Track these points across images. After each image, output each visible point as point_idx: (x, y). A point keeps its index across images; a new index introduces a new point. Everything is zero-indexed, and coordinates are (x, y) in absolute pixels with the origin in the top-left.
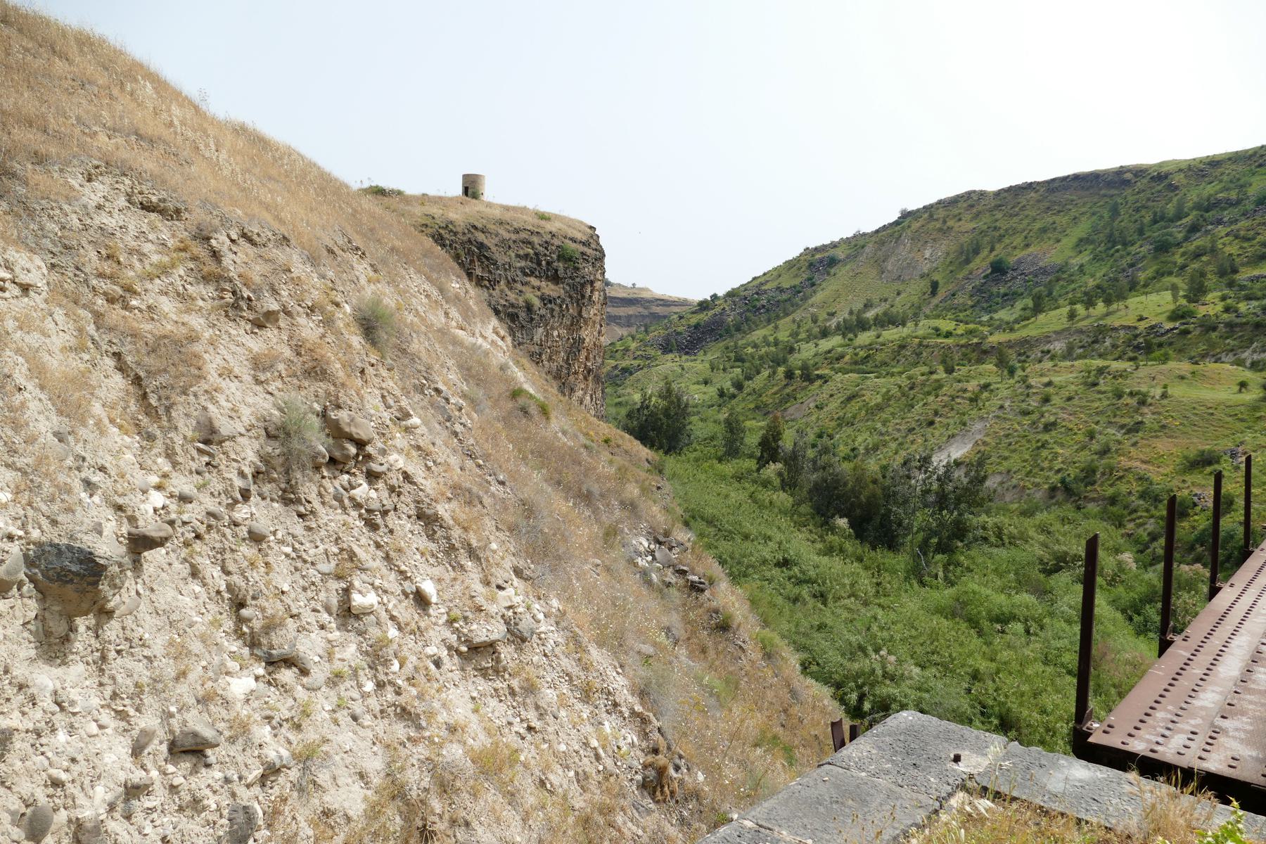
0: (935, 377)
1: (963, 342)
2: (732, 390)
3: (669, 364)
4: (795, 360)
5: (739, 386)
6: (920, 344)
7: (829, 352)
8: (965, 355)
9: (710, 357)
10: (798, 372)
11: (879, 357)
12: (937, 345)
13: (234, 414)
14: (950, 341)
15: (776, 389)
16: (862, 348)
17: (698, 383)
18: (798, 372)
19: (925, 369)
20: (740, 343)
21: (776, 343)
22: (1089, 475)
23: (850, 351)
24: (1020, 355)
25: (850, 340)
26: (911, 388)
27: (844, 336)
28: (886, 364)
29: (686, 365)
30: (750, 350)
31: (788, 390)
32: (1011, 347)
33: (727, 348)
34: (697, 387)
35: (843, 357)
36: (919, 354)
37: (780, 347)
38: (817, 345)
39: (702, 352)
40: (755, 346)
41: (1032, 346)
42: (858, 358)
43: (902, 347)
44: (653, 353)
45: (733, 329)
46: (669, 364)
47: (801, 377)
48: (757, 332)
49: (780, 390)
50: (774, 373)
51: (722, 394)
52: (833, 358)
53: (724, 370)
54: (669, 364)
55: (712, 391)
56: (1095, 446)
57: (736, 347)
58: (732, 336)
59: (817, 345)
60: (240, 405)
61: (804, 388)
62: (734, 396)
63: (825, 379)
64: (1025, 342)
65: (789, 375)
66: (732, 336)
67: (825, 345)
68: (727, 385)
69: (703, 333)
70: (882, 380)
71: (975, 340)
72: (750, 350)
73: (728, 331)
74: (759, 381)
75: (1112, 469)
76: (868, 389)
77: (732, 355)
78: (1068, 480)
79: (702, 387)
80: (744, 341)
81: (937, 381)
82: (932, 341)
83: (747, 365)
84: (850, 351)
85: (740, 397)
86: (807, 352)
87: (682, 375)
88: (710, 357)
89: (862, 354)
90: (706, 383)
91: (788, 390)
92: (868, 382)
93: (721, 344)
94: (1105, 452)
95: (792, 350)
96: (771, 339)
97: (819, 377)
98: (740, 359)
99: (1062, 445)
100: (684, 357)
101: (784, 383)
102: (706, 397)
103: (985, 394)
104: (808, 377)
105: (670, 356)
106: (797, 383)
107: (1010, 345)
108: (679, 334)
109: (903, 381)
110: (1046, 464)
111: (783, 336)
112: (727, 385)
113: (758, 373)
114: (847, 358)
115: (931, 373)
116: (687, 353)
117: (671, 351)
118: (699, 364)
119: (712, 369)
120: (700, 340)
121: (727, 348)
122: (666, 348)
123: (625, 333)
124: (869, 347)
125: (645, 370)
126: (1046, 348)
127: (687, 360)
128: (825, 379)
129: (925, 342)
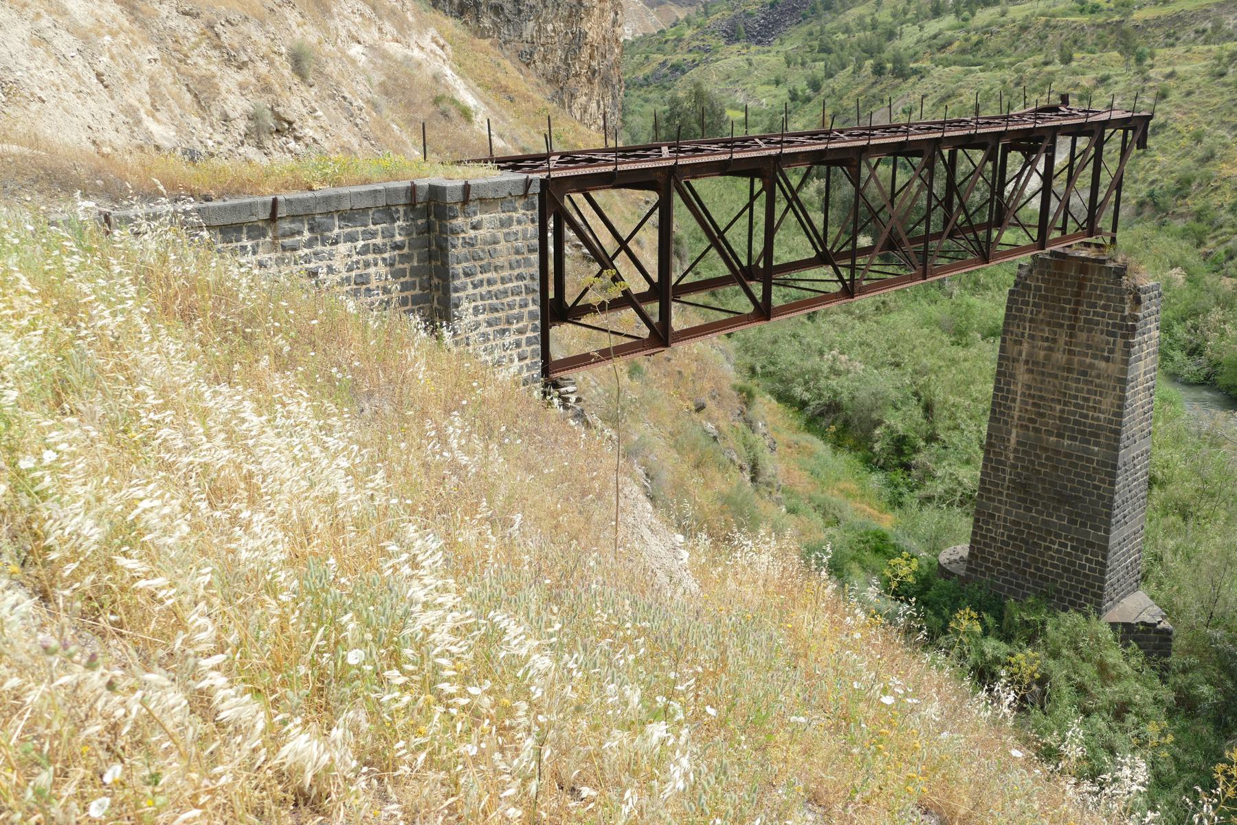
0: (1049, 68)
1: (1101, 19)
2: (809, 92)
3: (734, 58)
4: (890, 49)
5: (815, 86)
6: (1047, 25)
7: (935, 37)
8: (1100, 37)
9: (788, 47)
10: (889, 66)
11: (994, 42)
12: (1067, 25)
13: (234, 109)
14: (1084, 19)
15: (861, 88)
16: (976, 30)
17: (768, 83)
18: (889, 66)
19: (1040, 58)
20: (828, 27)
21: (874, 27)
22: (1183, 187)
23: (962, 35)
24: (1168, 36)
25: (965, 20)
26: (1018, 84)
27: (958, 13)
28: (1000, 52)
29: (755, 59)
30: (841, 37)
31: (875, 90)
32: (1159, 26)
33: (811, 34)
34: (767, 88)
35: (950, 44)
36: (1043, 38)
37: (879, 31)
38: (921, 28)
39: (778, 41)
40: (847, 30)
41: (1185, 24)
42: (965, 45)
43: (1024, 29)
44: (713, 42)
45: (820, 7)
46: (734, 58)
47: (893, 71)
48: (853, 11)
49: (865, 91)
50: (860, 68)
51: (794, 97)
52: (939, 45)
53: (803, 64)
54: (733, 57)
55: (783, 93)
56: (1199, 152)
57: (822, 32)
58: (819, 17)
59: (921, 28)
60: (237, 105)
61: (896, 87)
62: (808, 100)
63: (920, 74)
64: (1178, 18)
65: (879, 70)
66: (819, 17)
67: (932, 27)
68: (802, 86)
69: (782, 13)
70: (988, 74)
71: (1117, 18)
72: (841, 37)
73: (814, 10)
74: (842, 78)
75: (1209, 179)
76: (968, 86)
77: (816, 43)
78: (1157, 192)
79: (773, 88)
80: (834, 24)
81: (1052, 73)
82: (1061, 20)
83: (833, 56)
84: (962, 35)
85: (814, 102)
86: (910, 37)
87: (749, 73)
88: (788, 47)
89: (975, 38)
90: (777, 83)
91: (875, 90)
92: (970, 78)
93: (805, 29)
94: (1209, 157)
95: (891, 35)
96: (868, 20)
97: (915, 72)
98: (825, 50)
99: (1164, 151)
100: (754, 48)
101: (872, 80)
102: (776, 102)
103: (1101, 90)
104: (901, 73)
105: (738, 46)
106: (888, 80)
107: (1158, 23)
108: (750, 15)
109: (1009, 75)
110: (1140, 176)
111: (884, 16)
112: (802, 86)
113: (844, 67)
114: (957, 44)
115: (1046, 64)
116: (759, 42)
117: (738, 40)
118: (770, 58)
119: (789, 63)
120: (777, 23)
121: (811, 34)
122: (732, 36)
123: (681, 17)
124: (987, 30)
125: (702, 67)
126: (1201, 27)
127: (758, 52)
128: (920, 74)
129: (1053, 22)
